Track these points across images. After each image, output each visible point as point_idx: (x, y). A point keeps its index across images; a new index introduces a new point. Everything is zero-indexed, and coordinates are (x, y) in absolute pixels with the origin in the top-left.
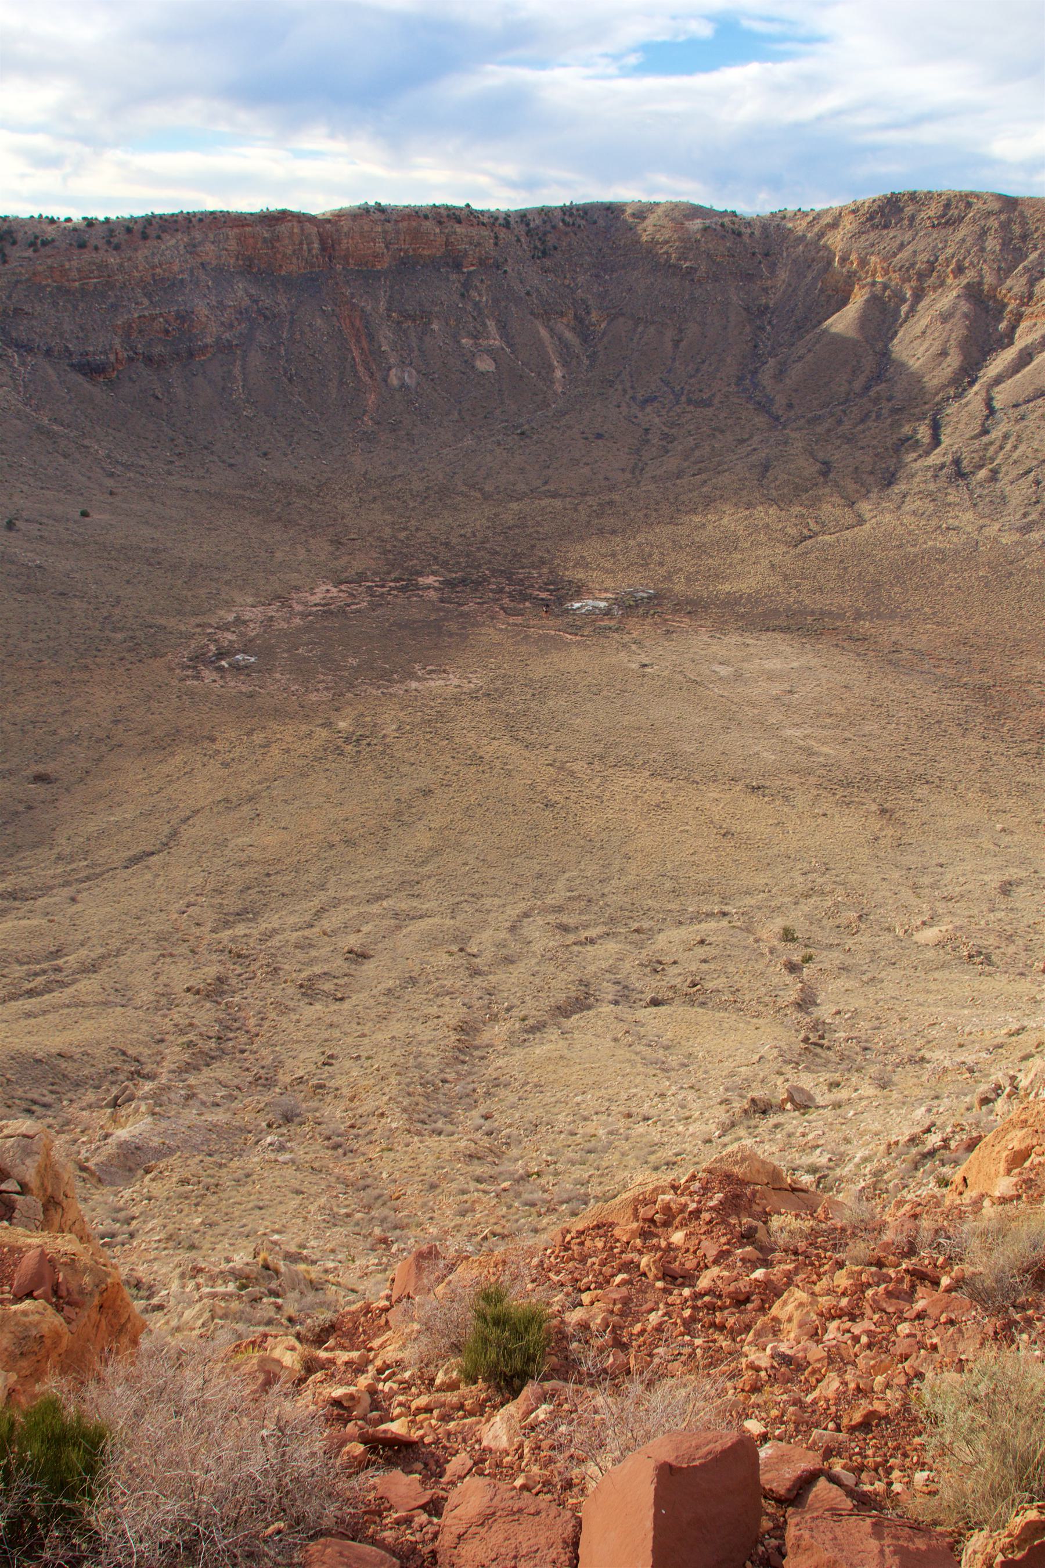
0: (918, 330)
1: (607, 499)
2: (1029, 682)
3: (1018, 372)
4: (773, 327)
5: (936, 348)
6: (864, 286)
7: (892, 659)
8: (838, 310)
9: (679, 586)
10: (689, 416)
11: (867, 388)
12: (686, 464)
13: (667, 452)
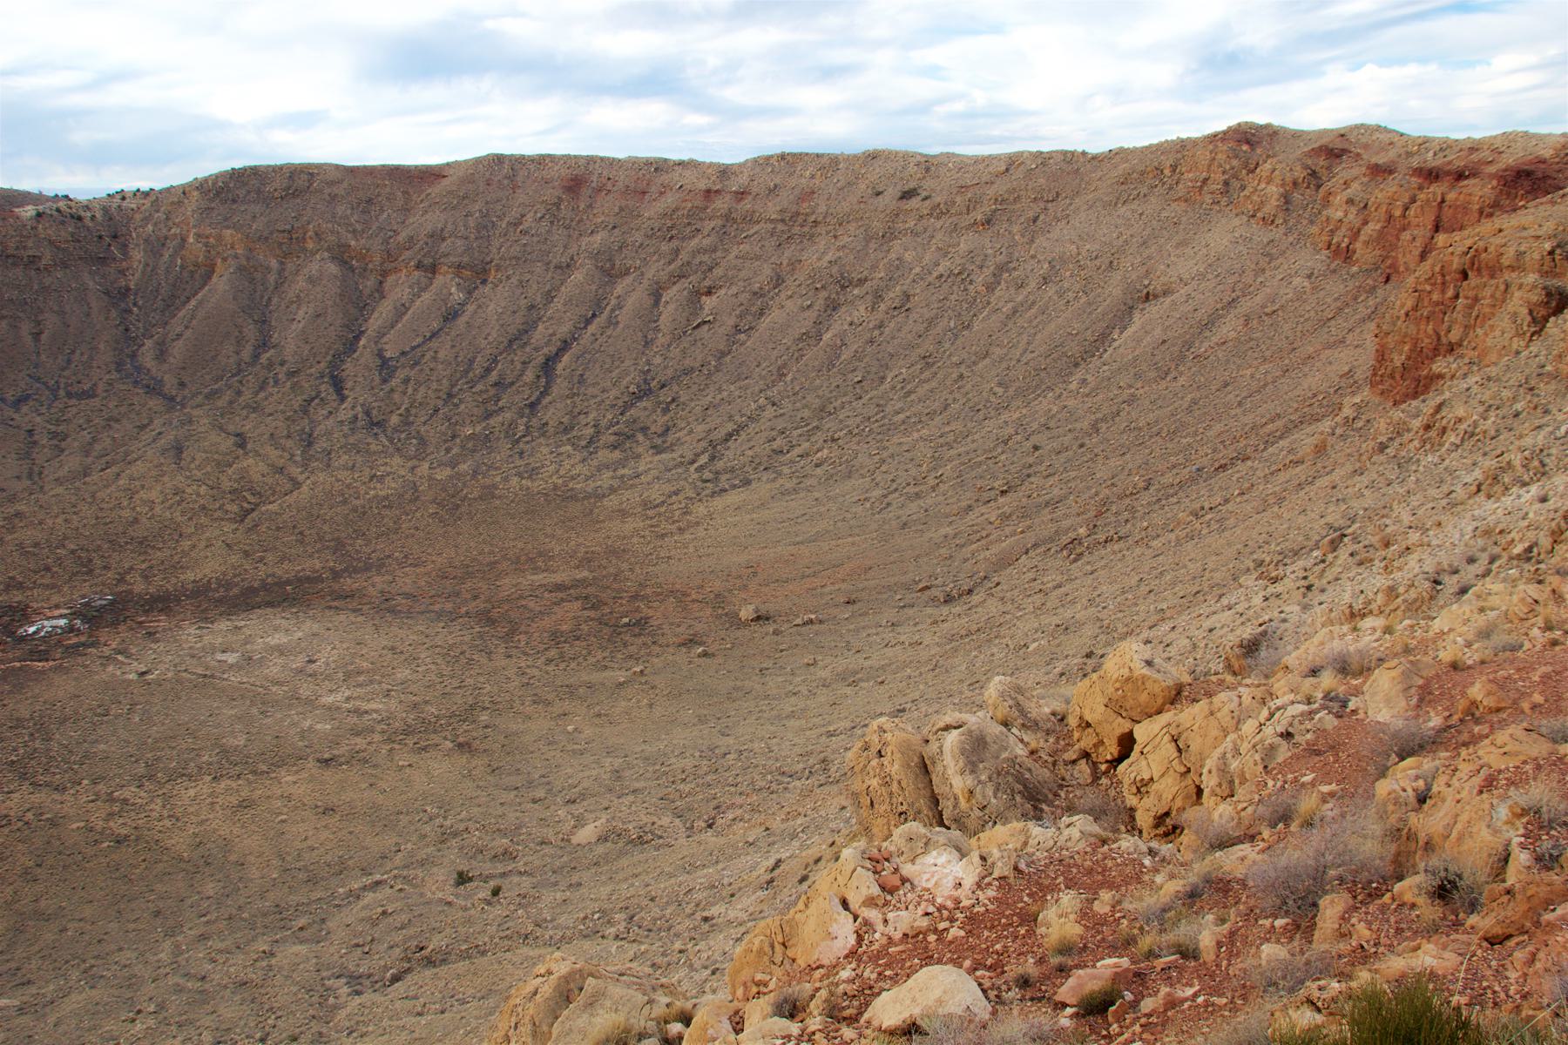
0: (291, 295)
1: (12, 511)
2: (521, 597)
4: (140, 308)
6: (225, 260)
7: (387, 607)
8: (205, 284)
9: (139, 587)
10: (74, 410)
11: (256, 357)
12: (90, 460)
13: (63, 451)
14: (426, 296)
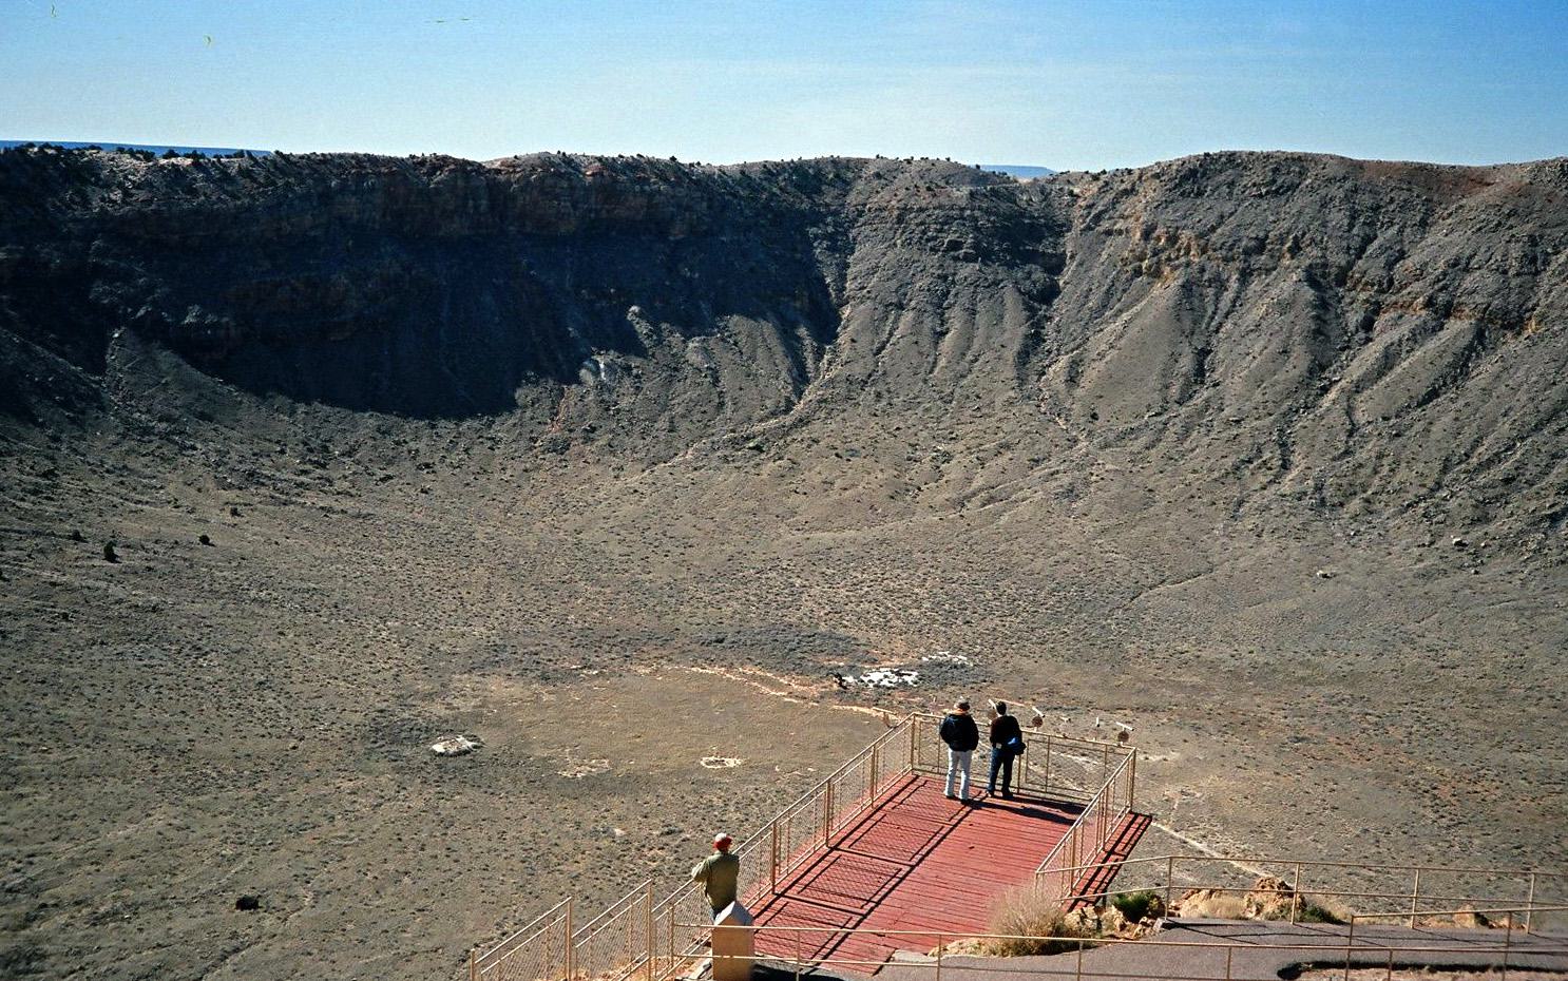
3: (1384, 374)
5: (1275, 345)
6: (1176, 268)
14: (1432, 345)
